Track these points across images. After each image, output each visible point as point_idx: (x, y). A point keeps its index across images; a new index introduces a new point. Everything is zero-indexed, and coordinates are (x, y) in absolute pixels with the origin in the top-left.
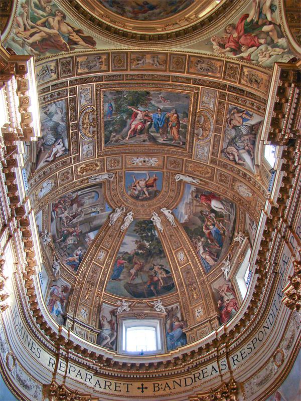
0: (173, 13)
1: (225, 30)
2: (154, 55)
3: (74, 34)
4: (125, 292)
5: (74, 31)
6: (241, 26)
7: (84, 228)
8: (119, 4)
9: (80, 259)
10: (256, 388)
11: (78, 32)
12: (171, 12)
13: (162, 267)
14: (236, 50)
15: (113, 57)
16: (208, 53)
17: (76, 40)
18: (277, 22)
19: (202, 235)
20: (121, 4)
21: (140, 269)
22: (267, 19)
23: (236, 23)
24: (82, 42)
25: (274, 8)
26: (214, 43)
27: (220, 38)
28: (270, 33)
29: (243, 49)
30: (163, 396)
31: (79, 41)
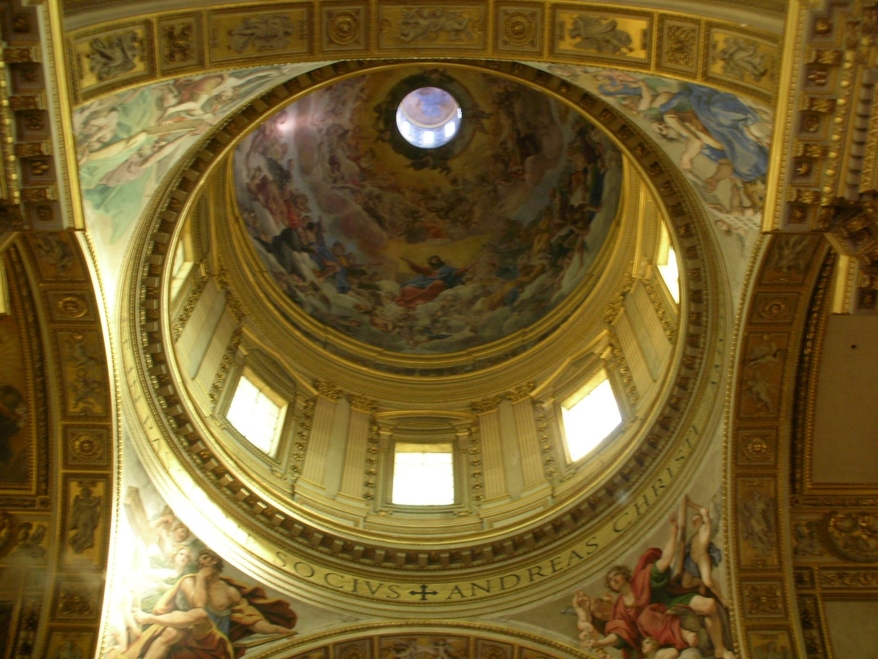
0: (507, 309)
1: (608, 580)
2: (438, 640)
3: (244, 605)
5: (244, 596)
6: (643, 579)
8: (363, 273)
12: (503, 302)
15: (338, 651)
16: (564, 640)
17: (247, 620)
18: (722, 596)
20: (370, 272)
22: (700, 577)
23: (633, 566)
24: (263, 624)
25: (715, 555)
26: (581, 613)
27: (596, 602)
28: (708, 621)
31: (257, 621)
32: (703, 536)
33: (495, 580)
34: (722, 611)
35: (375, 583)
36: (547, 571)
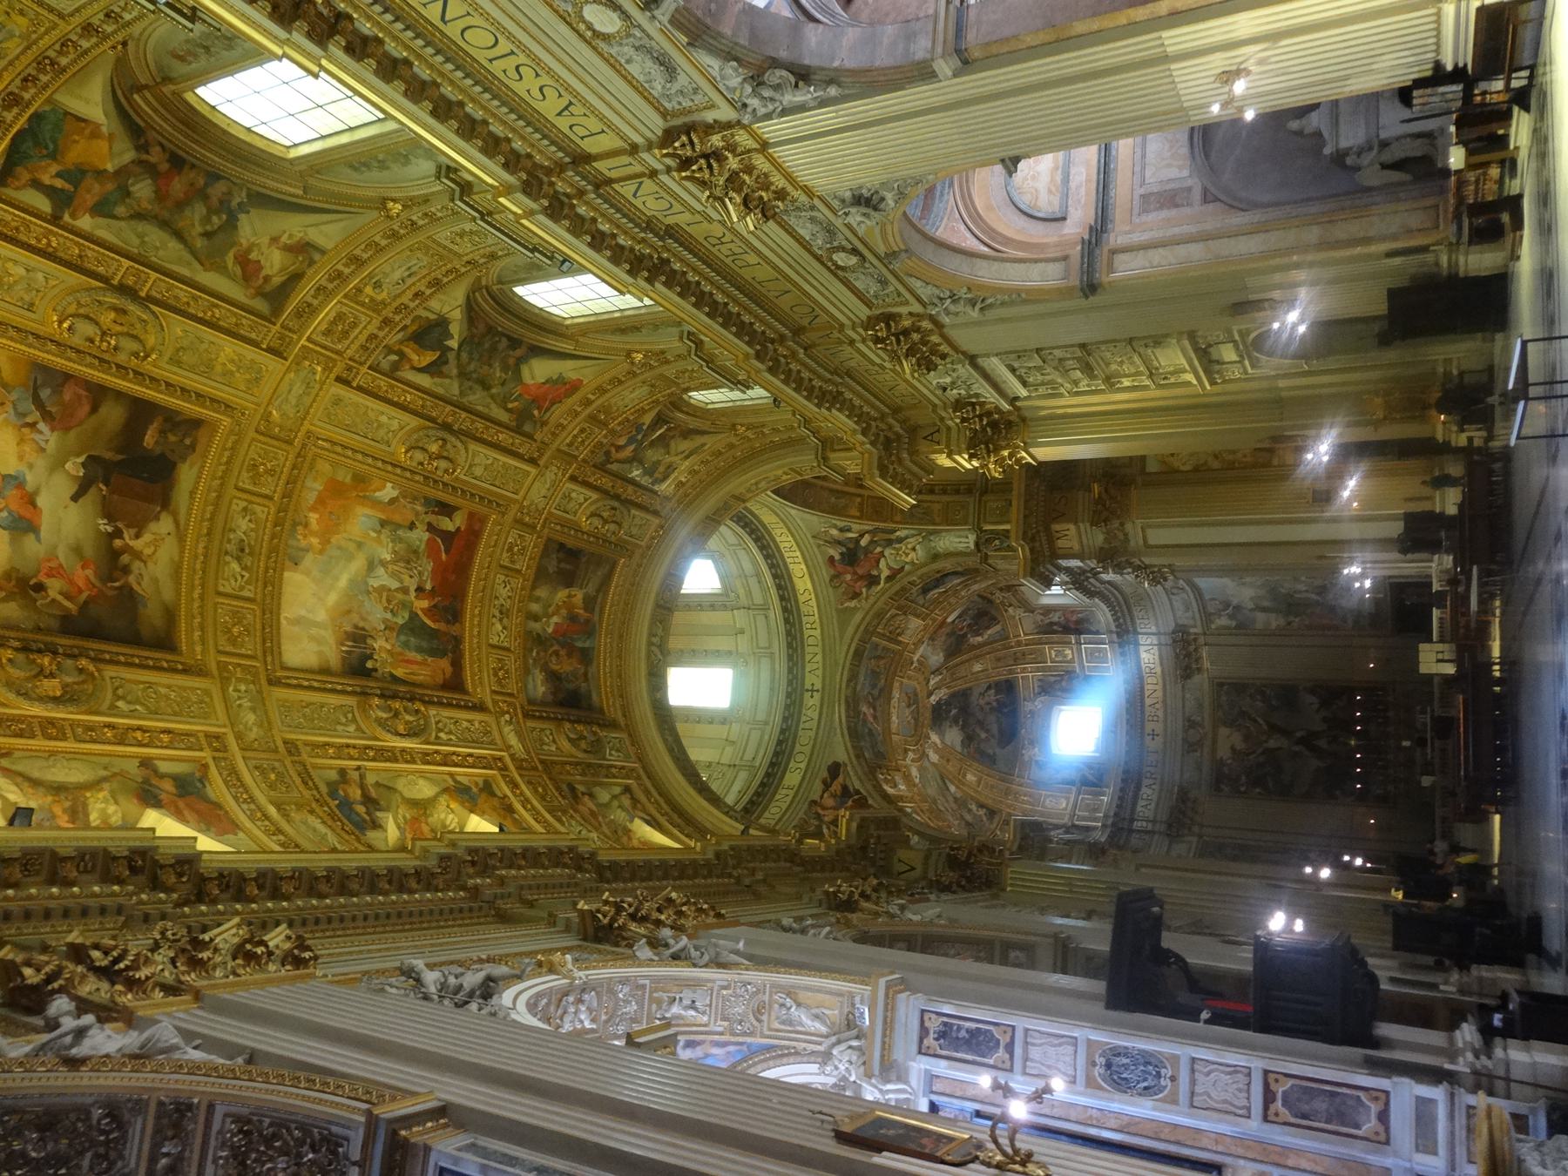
3: (832, 789)
4: (1009, 748)
6: (840, 567)
7: (951, 799)
9: (981, 806)
10: (1190, 614)
11: (827, 785)
13: (982, 694)
14: (873, 581)
16: (858, 617)
19: (965, 635)
21: (981, 724)
23: (832, 572)
24: (840, 779)
29: (875, 573)
30: (1165, 711)
32: (834, 532)
33: (808, 649)
34: (873, 532)
35: (804, 718)
36: (811, 619)
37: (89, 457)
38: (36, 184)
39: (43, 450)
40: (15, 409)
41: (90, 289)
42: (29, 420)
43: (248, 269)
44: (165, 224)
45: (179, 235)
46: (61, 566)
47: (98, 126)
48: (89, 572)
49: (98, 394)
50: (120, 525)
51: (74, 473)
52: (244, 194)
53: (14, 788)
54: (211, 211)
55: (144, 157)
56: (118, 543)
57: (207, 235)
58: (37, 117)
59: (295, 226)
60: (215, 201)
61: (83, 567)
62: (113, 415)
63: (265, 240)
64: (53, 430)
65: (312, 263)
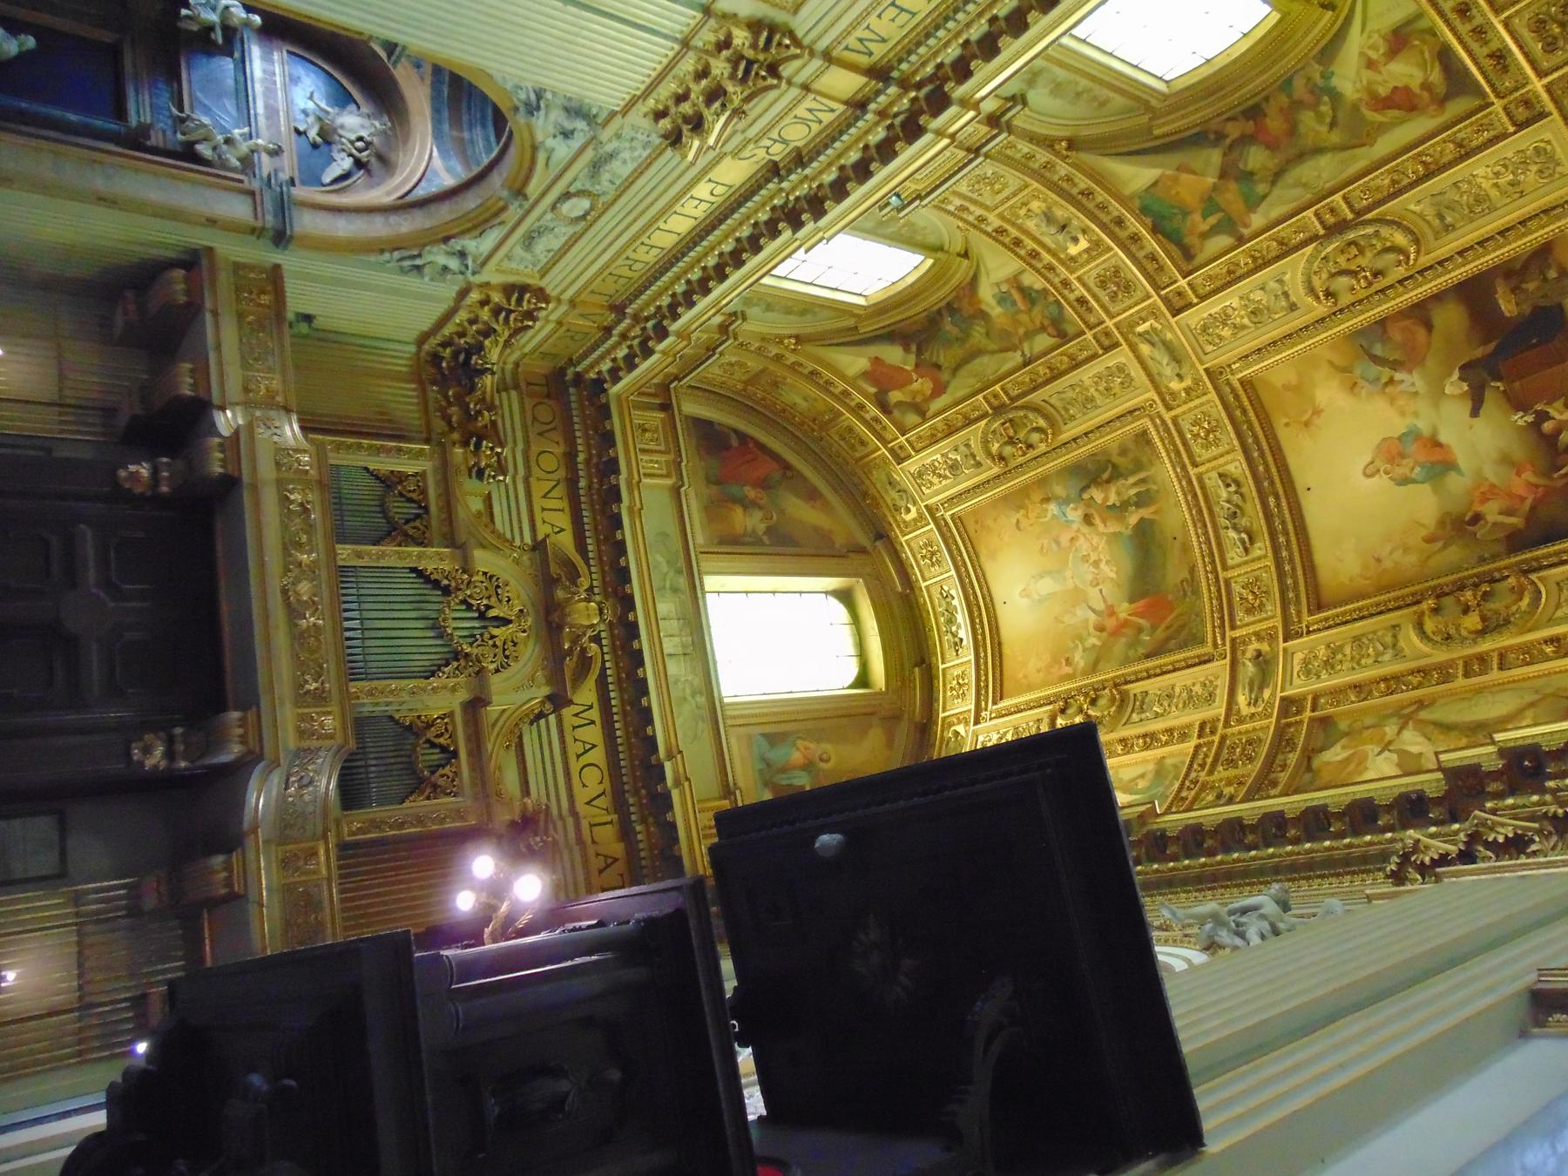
37: (1463, 368)
38: (1205, 236)
39: (1416, 393)
40: (1367, 380)
41: (1313, 256)
42: (1384, 380)
43: (1402, 102)
44: (1301, 157)
45: (1318, 151)
46: (1493, 486)
47: (1162, 175)
48: (1529, 476)
49: (1420, 313)
50: (1539, 407)
51: (1457, 392)
52: (1317, 66)
53: (1421, 739)
54: (1314, 106)
55: (1228, 141)
56: (1548, 426)
57: (1333, 124)
58: (1144, 211)
59: (1355, 41)
60: (1307, 97)
61: (1518, 474)
62: (1451, 318)
63: (1367, 75)
64: (1410, 372)
65: (1432, 32)
